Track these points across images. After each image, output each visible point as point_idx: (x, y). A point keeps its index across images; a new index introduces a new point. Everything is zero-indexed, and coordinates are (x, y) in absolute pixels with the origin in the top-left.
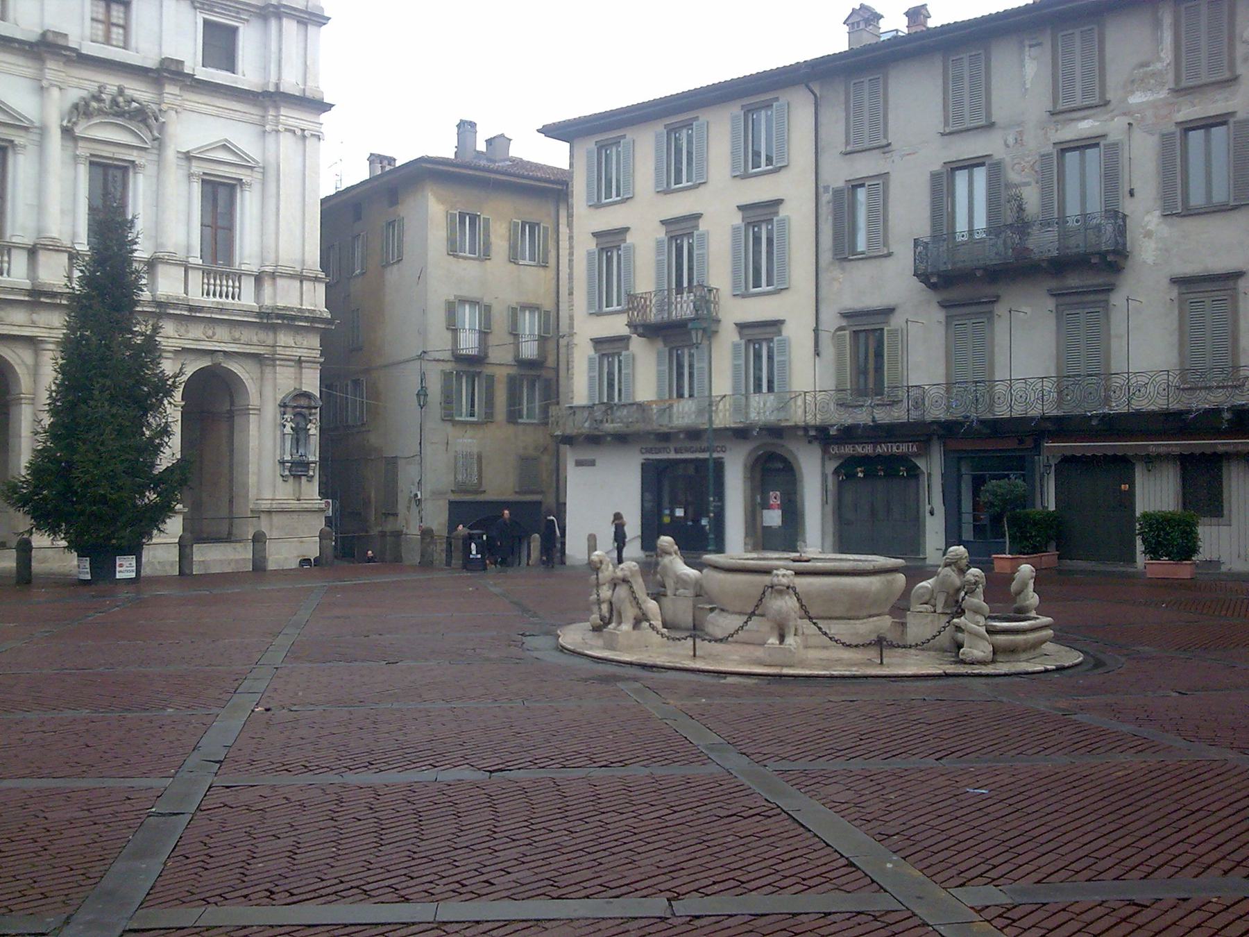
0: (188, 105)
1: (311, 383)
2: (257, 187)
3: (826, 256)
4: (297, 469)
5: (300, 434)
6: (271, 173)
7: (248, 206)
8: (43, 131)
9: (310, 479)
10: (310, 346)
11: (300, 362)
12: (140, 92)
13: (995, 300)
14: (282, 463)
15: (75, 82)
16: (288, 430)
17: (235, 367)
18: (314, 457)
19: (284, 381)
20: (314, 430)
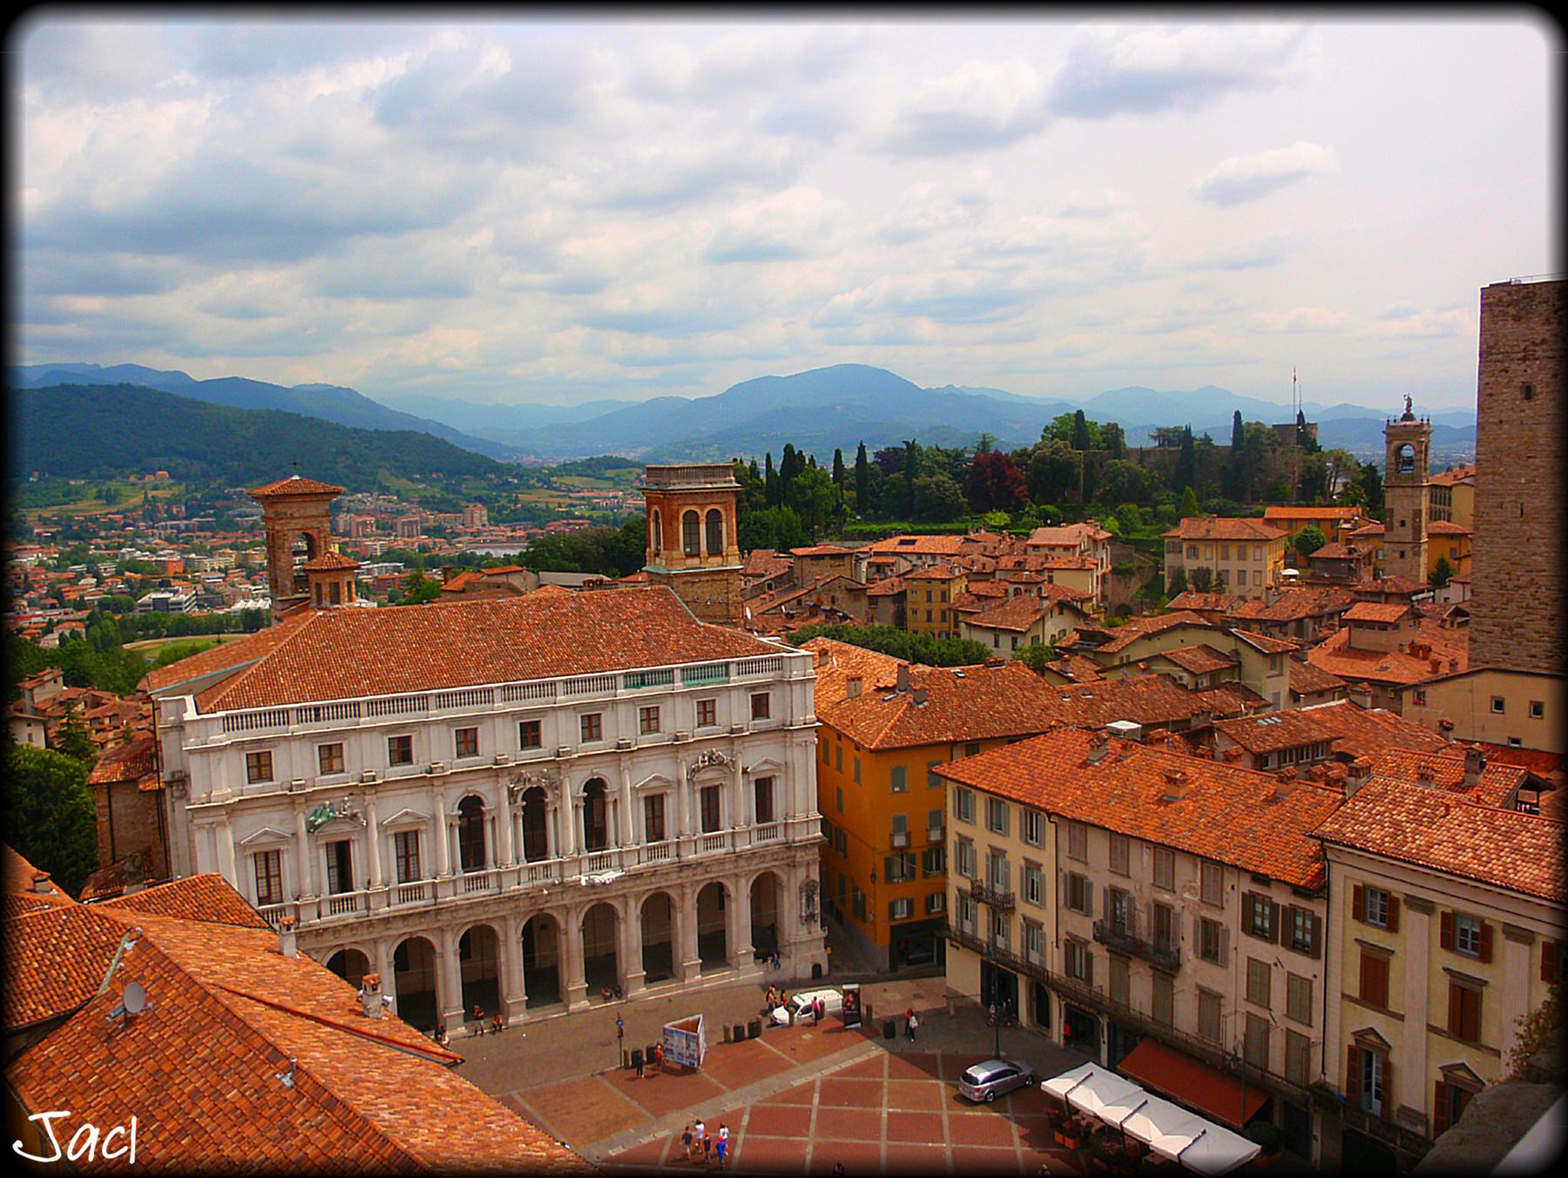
0: (746, 745)
1: (815, 876)
2: (783, 775)
3: (1061, 902)
4: (811, 917)
5: (810, 899)
6: (790, 767)
7: (778, 789)
8: (679, 783)
9: (816, 921)
10: (814, 854)
11: (808, 864)
12: (721, 752)
13: (1130, 958)
14: (801, 917)
15: (691, 752)
16: (804, 901)
17: (774, 870)
18: (818, 911)
19: (801, 874)
20: (817, 898)
